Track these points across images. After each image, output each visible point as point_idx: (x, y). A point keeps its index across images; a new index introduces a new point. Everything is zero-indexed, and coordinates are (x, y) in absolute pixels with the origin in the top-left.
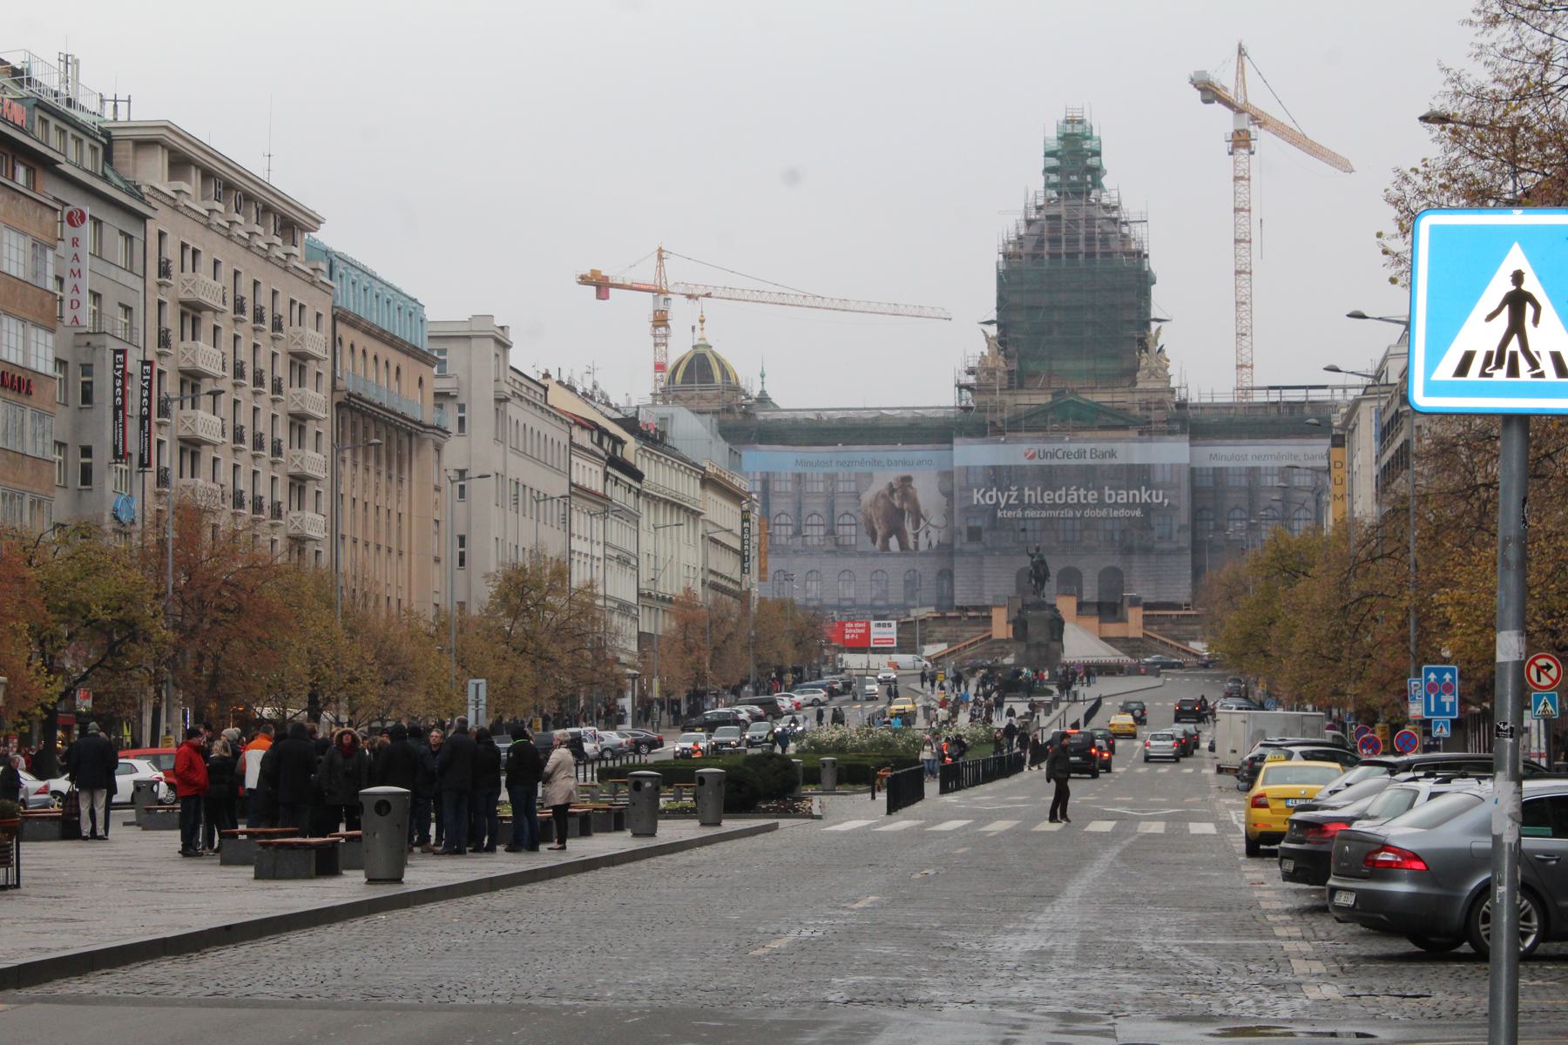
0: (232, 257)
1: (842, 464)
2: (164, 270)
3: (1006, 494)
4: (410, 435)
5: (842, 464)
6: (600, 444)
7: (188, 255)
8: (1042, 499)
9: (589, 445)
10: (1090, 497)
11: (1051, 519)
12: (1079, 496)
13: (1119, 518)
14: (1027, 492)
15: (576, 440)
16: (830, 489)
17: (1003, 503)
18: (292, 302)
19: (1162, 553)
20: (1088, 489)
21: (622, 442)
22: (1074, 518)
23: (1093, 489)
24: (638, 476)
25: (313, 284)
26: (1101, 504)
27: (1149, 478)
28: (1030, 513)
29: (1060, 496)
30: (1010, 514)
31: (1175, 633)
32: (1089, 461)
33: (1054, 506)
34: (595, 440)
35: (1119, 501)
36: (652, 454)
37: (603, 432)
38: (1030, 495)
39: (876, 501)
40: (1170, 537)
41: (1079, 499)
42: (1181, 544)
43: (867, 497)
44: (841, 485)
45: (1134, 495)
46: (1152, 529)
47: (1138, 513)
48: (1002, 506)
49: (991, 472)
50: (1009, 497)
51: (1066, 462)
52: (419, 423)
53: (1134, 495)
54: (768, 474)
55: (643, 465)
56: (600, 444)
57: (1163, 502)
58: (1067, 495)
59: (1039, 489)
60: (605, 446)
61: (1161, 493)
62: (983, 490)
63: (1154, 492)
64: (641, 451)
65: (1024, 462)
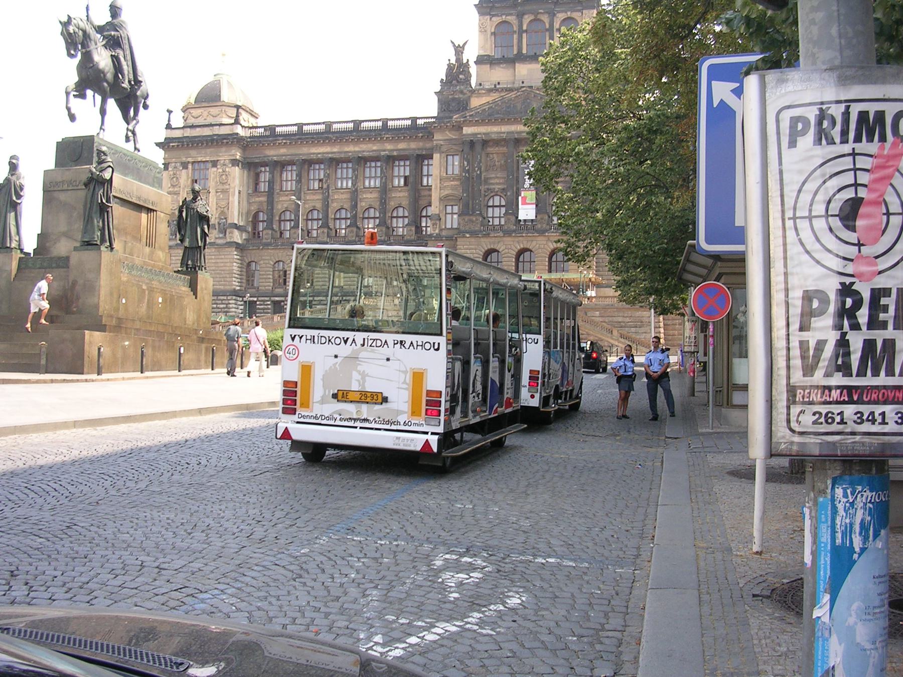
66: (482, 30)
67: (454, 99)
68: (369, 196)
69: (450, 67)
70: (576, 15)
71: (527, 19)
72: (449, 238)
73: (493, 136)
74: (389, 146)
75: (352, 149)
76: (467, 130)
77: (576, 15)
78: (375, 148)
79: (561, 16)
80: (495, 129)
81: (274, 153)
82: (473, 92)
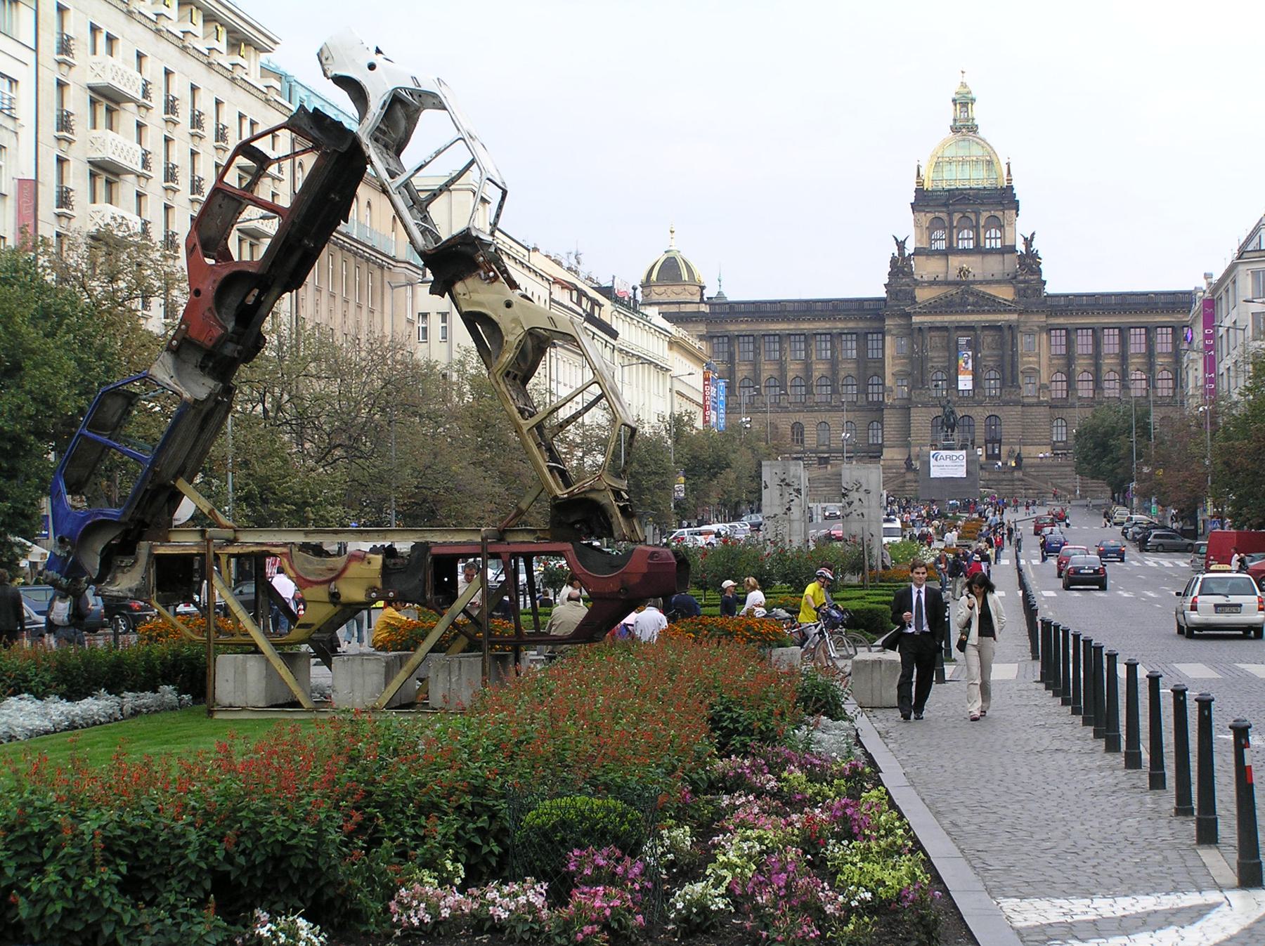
0: (162, 55)
2: (65, 46)
4: (382, 267)
6: (579, 304)
7: (101, 39)
9: (567, 302)
15: (556, 297)
18: (241, 117)
21: (600, 306)
24: (614, 335)
25: (267, 101)
34: (575, 299)
36: (625, 316)
37: (582, 293)
52: (393, 259)
55: (616, 325)
56: (580, 305)
60: (584, 306)
64: (616, 313)
66: (917, 224)
67: (900, 291)
68: (821, 366)
69: (894, 262)
70: (999, 214)
71: (957, 216)
72: (902, 408)
73: (938, 325)
74: (840, 325)
75: (806, 326)
76: (915, 319)
77: (999, 214)
78: (828, 326)
79: (985, 215)
80: (939, 318)
81: (733, 328)
82: (917, 283)
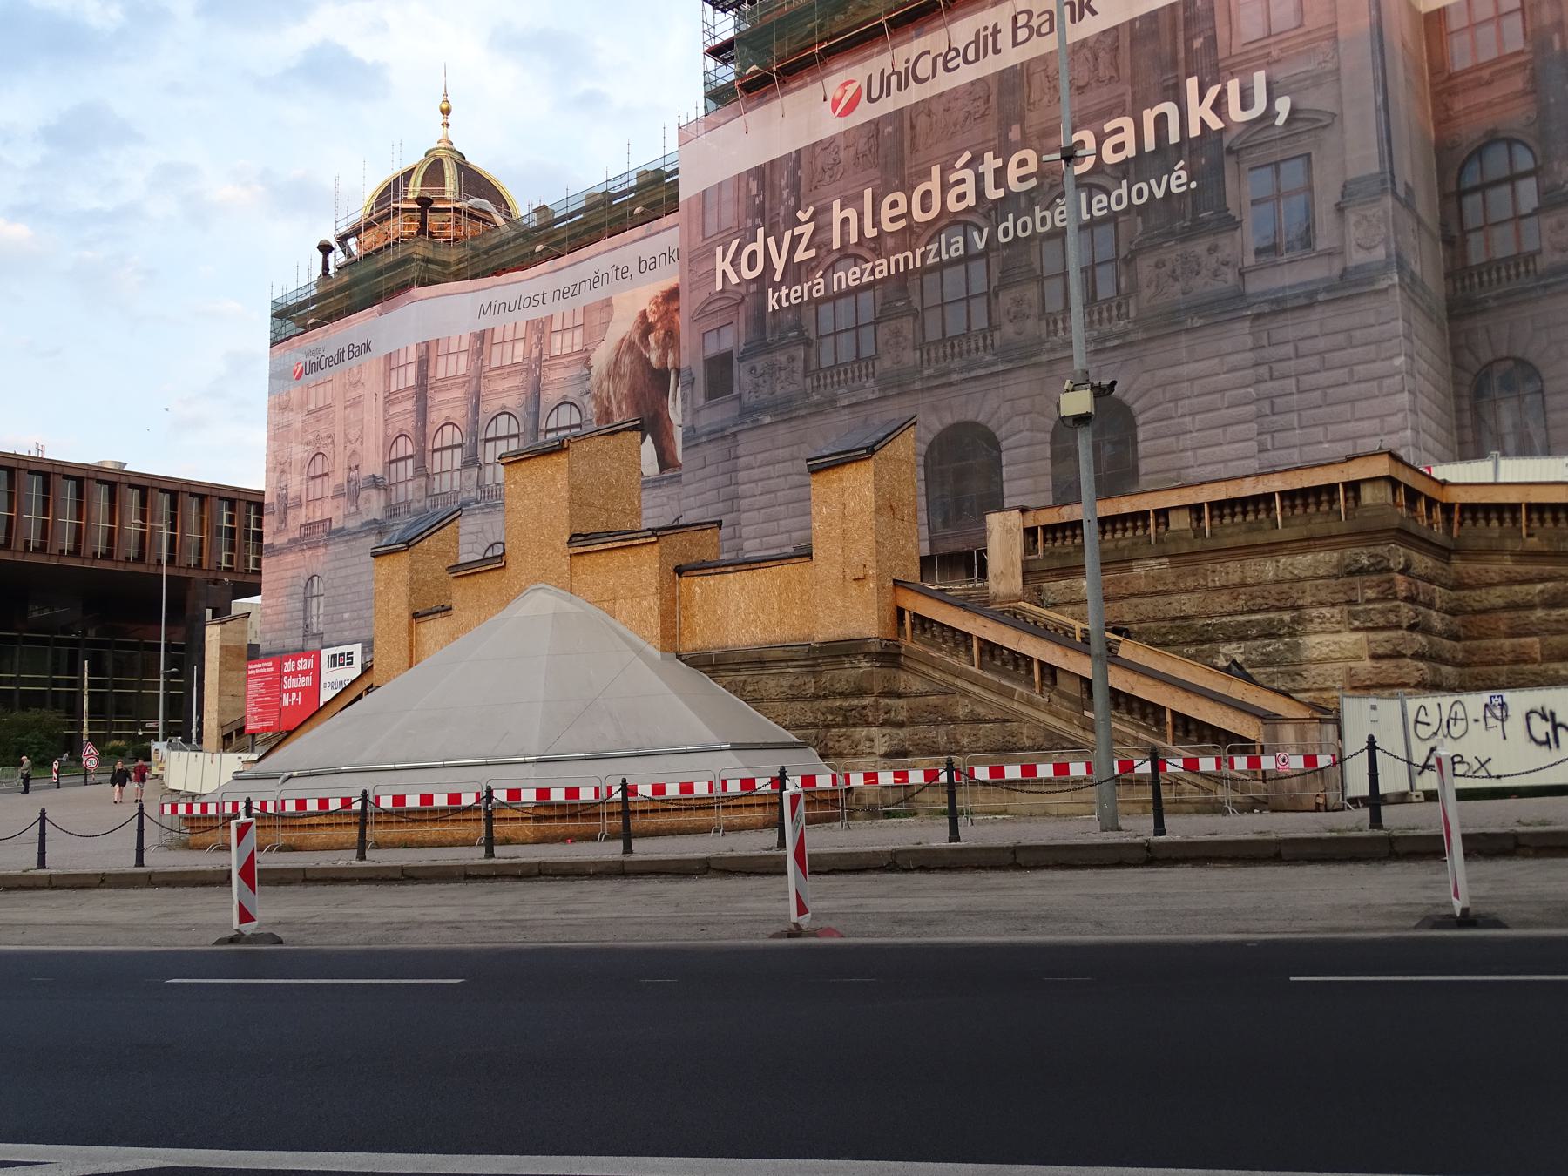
1: (562, 294)
3: (788, 235)
5: (562, 294)
8: (876, 223)
10: (1013, 173)
11: (901, 280)
12: (979, 178)
13: (1112, 218)
14: (837, 215)
16: (535, 353)
17: (779, 264)
19: (1280, 307)
20: (1004, 151)
22: (967, 258)
23: (1025, 143)
26: (1047, 188)
27: (1212, 41)
28: (848, 276)
29: (927, 194)
30: (797, 293)
31: (1186, 604)
32: (1011, 57)
33: (911, 234)
35: (1109, 157)
38: (845, 221)
39: (617, 362)
40: (1307, 239)
41: (980, 193)
42: (1357, 257)
43: (602, 356)
44: (557, 339)
45: (1161, 120)
46: (1233, 224)
47: (1178, 180)
48: (777, 278)
49: (754, 185)
50: (796, 240)
51: (945, 82)
53: (1161, 120)
54: (427, 344)
57: (1270, 113)
58: (945, 187)
59: (868, 193)
61: (1259, 78)
62: (735, 243)
63: (1233, 86)
65: (831, 125)
